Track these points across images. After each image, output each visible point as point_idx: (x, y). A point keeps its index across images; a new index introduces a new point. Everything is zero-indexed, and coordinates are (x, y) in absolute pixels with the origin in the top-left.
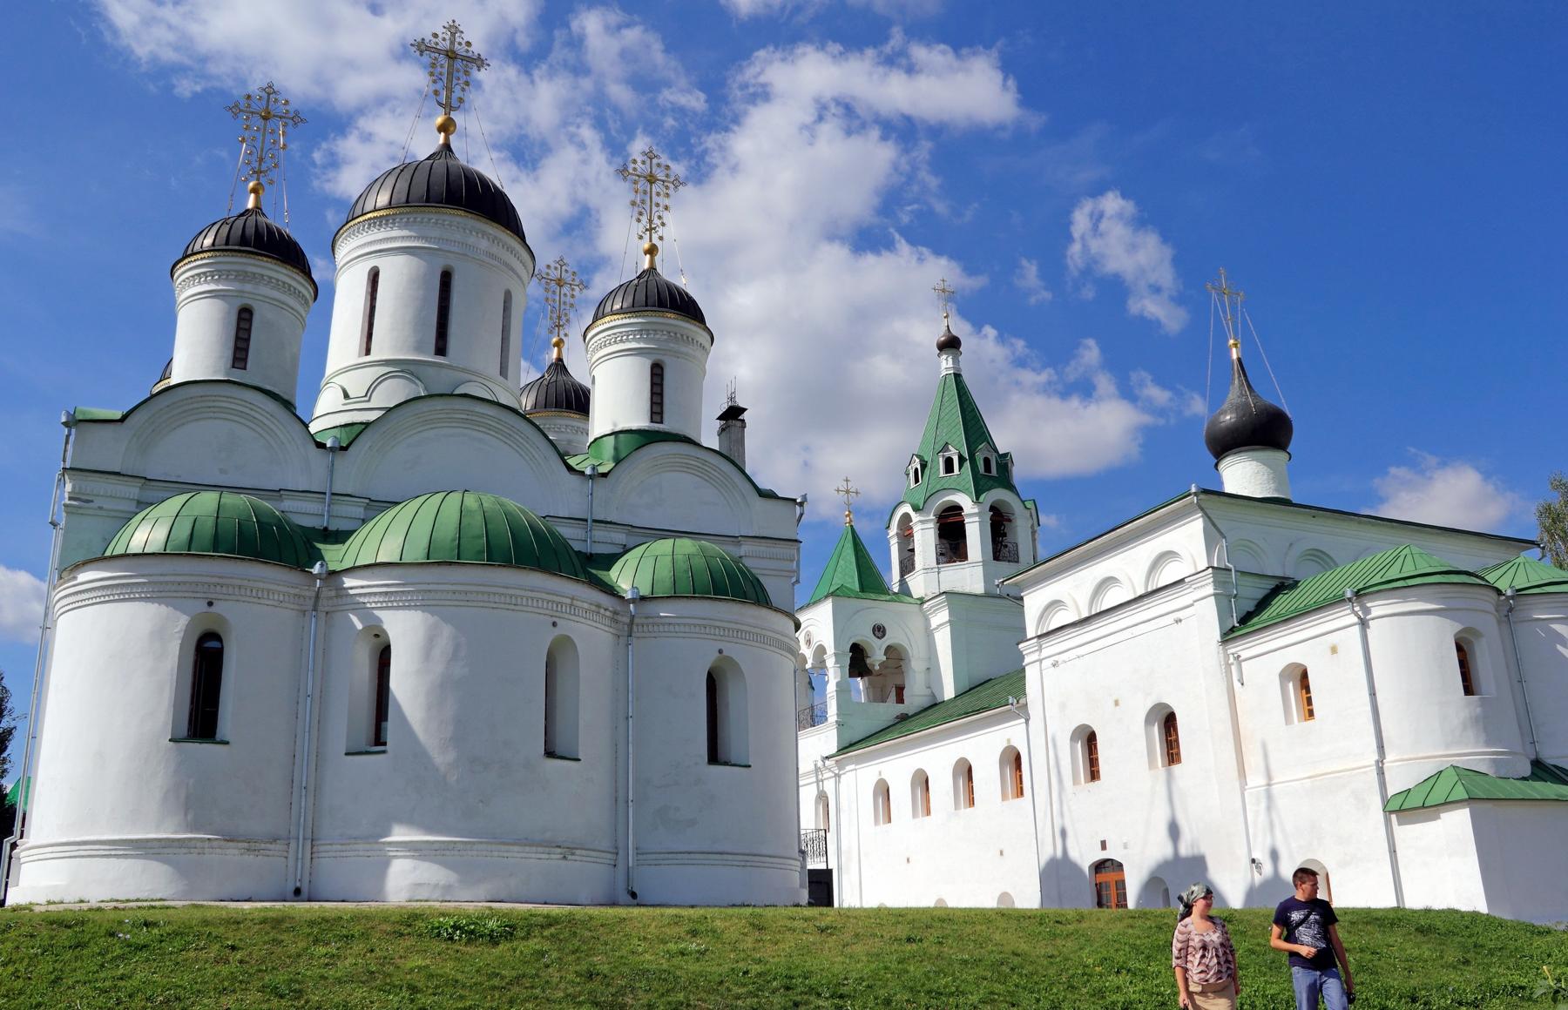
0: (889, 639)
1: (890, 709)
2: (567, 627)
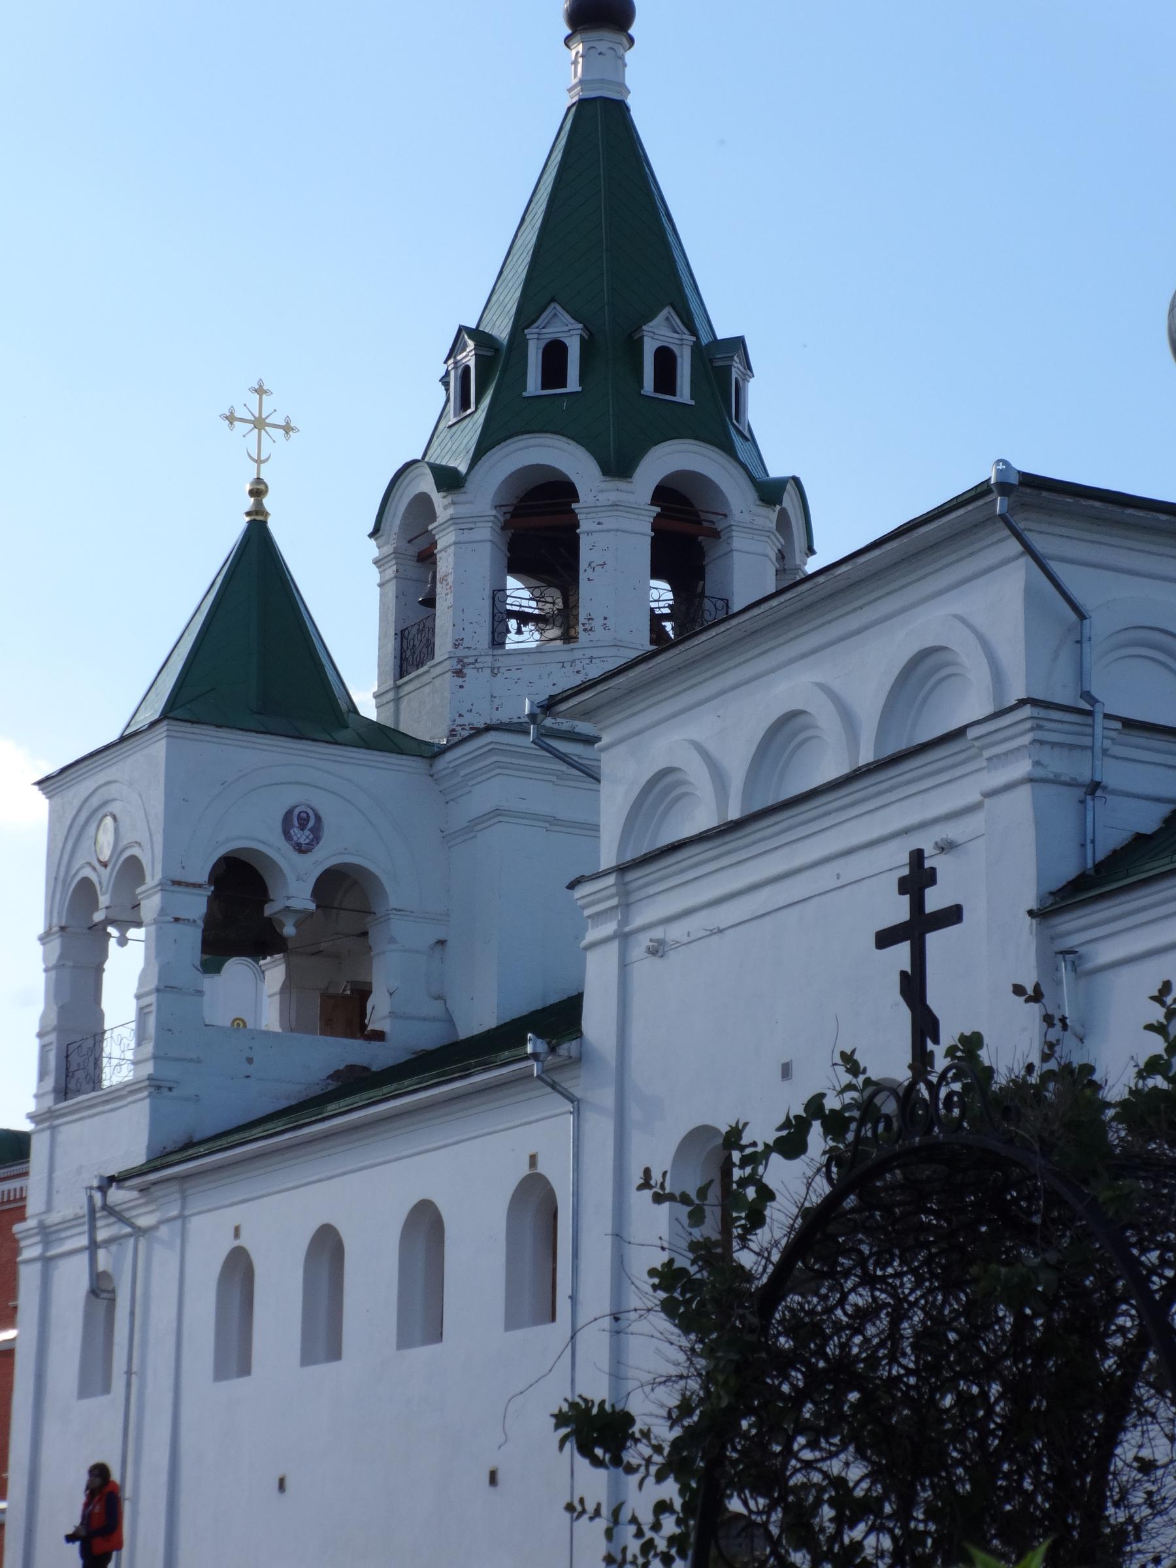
0: (324, 857)
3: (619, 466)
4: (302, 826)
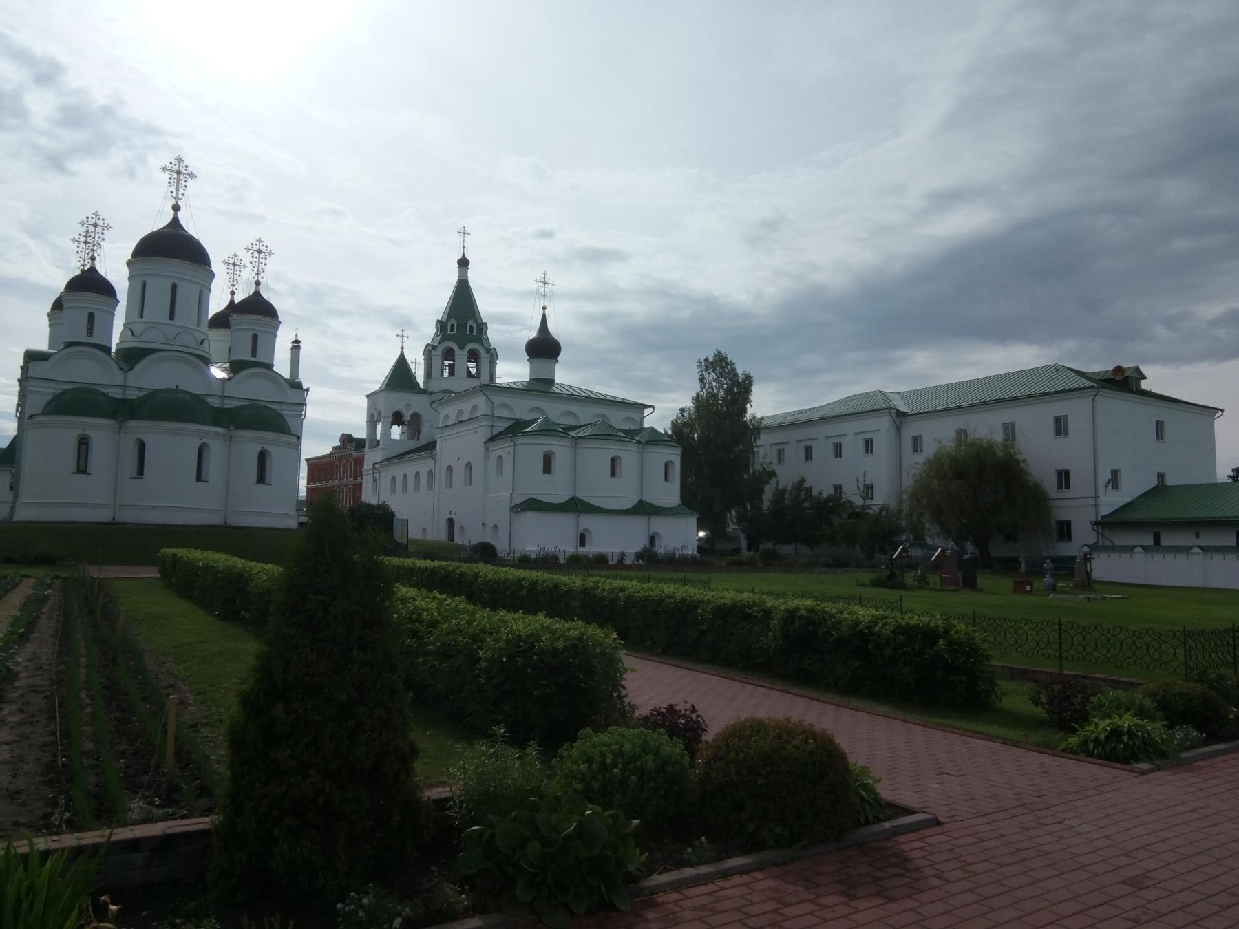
1: (414, 444)
2: (205, 441)
3: (462, 347)
4: (408, 405)
